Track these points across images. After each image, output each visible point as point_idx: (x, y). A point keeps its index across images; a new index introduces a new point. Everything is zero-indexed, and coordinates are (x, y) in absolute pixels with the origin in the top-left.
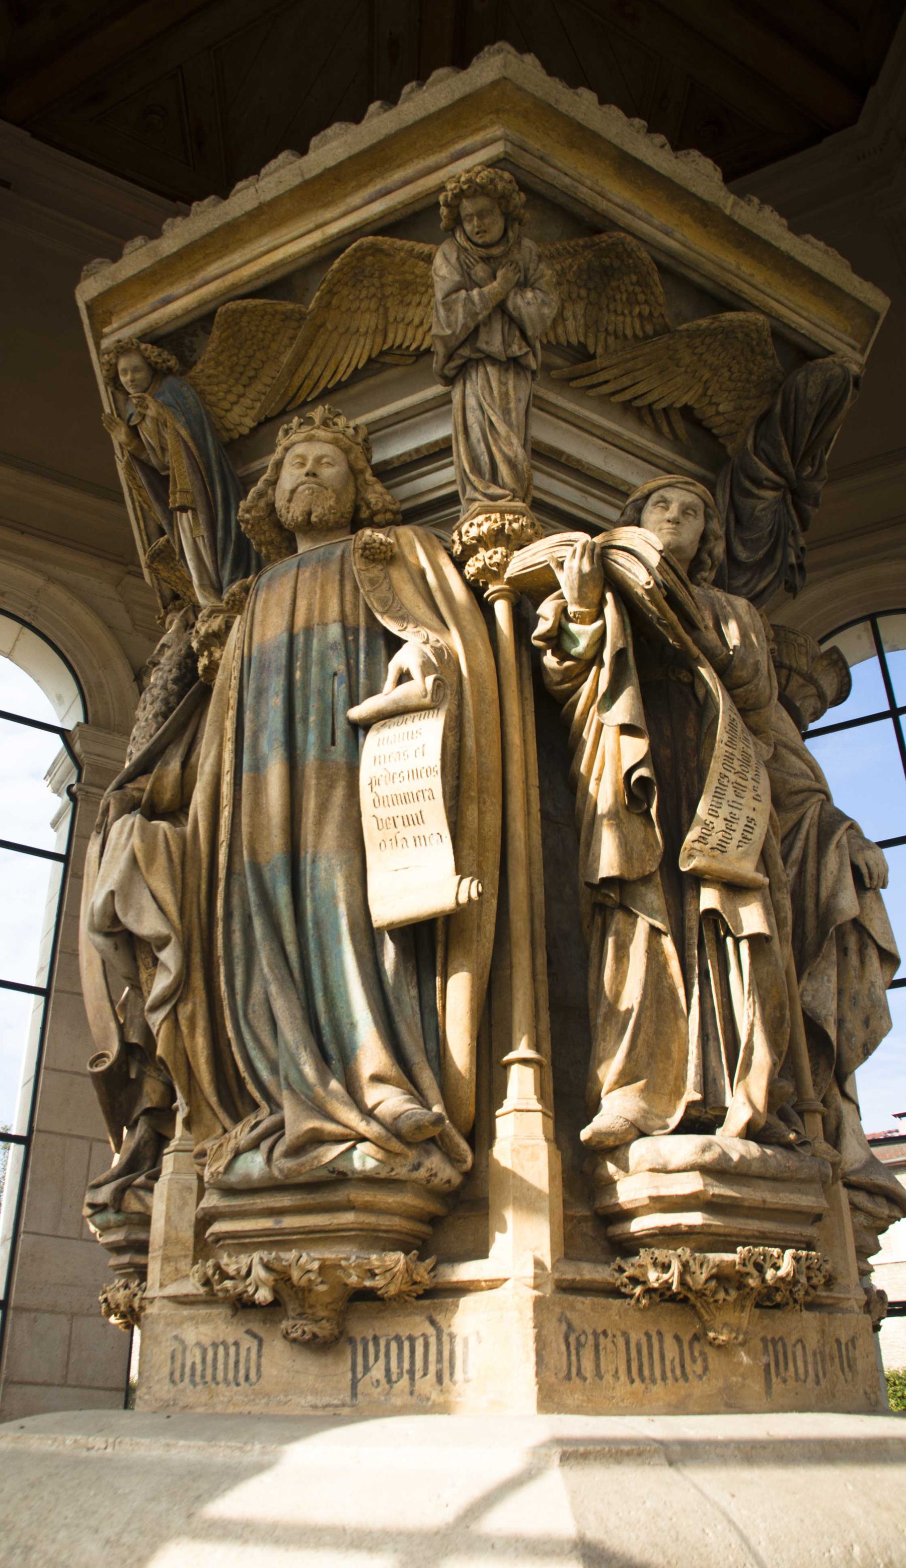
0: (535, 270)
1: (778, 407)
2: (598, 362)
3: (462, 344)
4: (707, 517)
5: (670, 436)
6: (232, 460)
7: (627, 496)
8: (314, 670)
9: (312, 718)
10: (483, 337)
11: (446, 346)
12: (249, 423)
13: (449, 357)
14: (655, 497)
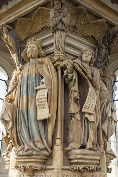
1: (106, 36)
2: (78, 29)
4: (92, 55)
6: (20, 46)
7: (81, 50)
8: (31, 81)
9: (30, 89)
10: (58, 26)
12: (24, 38)
13: (53, 29)
14: (84, 52)
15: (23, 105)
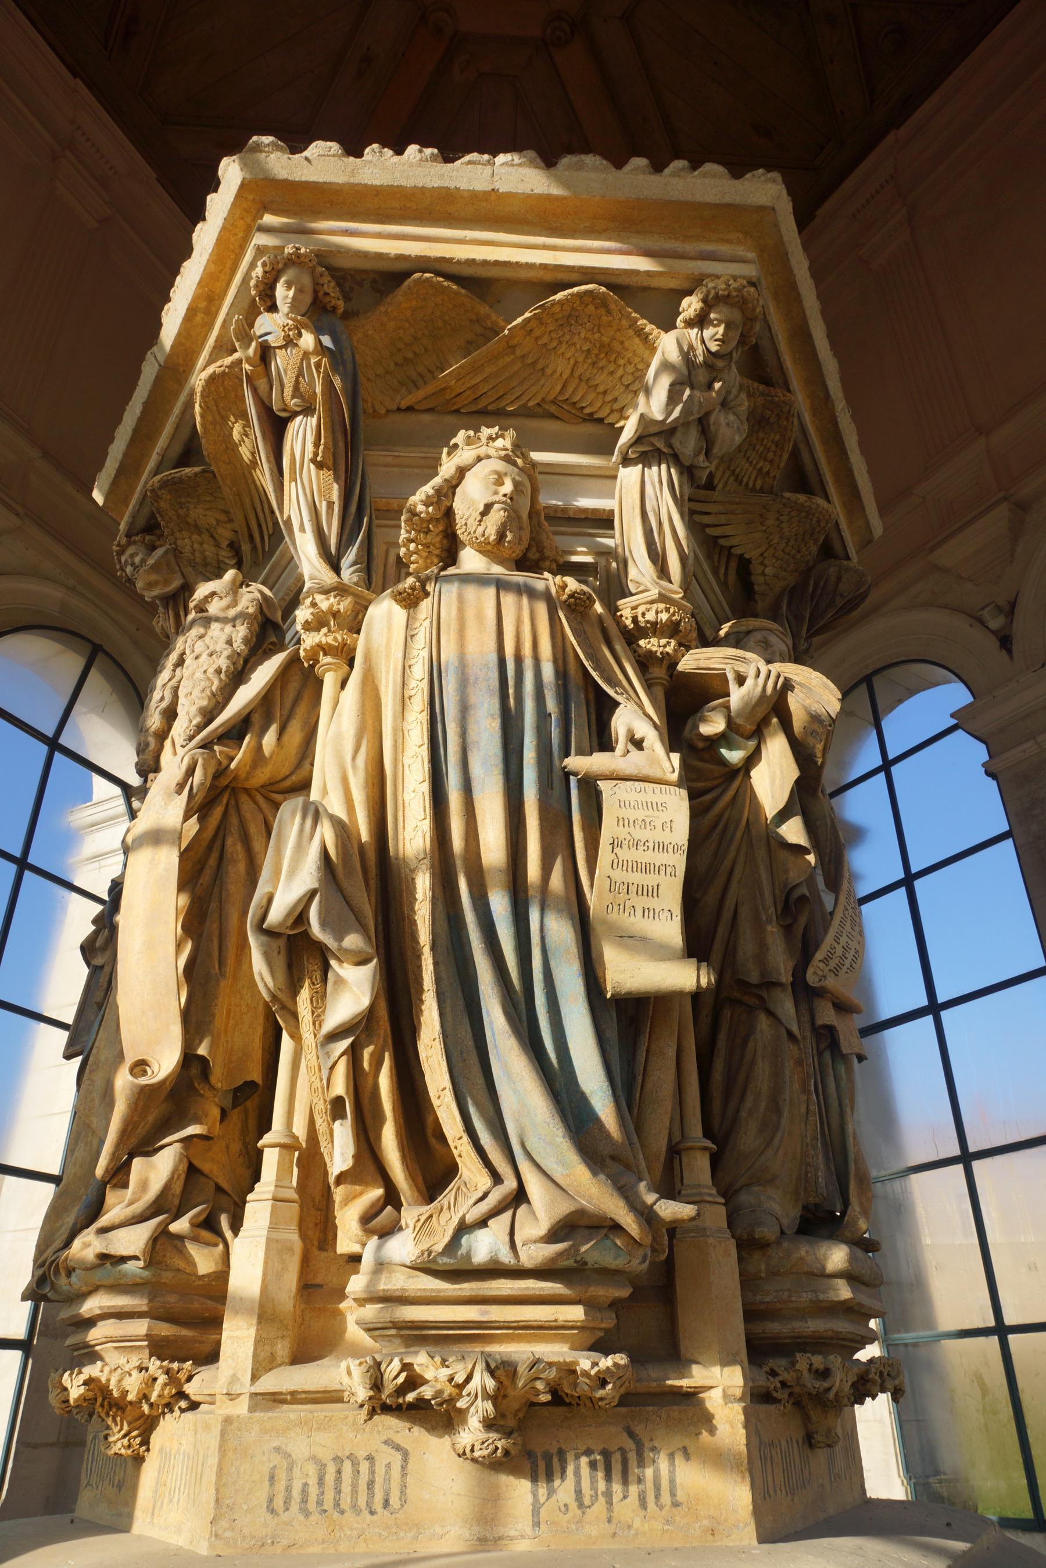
0: (737, 397)
2: (716, 495)
5: (722, 577)
10: (679, 434)
14: (758, 636)
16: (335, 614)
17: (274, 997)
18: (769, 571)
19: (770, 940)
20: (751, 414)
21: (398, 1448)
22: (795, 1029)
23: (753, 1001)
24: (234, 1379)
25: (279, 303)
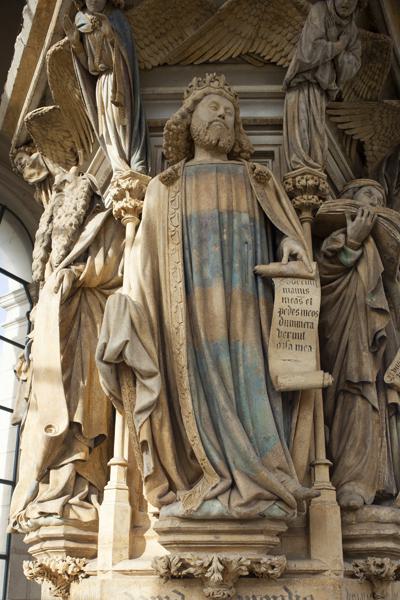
3: (308, 71)
10: (320, 71)
11: (300, 68)
15: (208, 321)
16: (130, 190)
17: (110, 393)
18: (375, 148)
19: (364, 360)
20: (364, 52)
21: (179, 594)
22: (376, 405)
23: (355, 391)
24: (105, 565)
25: (87, 5)
